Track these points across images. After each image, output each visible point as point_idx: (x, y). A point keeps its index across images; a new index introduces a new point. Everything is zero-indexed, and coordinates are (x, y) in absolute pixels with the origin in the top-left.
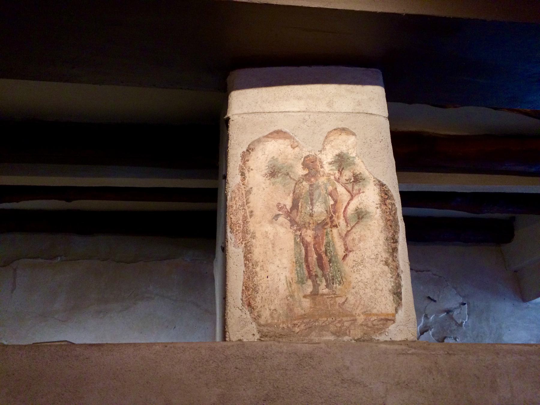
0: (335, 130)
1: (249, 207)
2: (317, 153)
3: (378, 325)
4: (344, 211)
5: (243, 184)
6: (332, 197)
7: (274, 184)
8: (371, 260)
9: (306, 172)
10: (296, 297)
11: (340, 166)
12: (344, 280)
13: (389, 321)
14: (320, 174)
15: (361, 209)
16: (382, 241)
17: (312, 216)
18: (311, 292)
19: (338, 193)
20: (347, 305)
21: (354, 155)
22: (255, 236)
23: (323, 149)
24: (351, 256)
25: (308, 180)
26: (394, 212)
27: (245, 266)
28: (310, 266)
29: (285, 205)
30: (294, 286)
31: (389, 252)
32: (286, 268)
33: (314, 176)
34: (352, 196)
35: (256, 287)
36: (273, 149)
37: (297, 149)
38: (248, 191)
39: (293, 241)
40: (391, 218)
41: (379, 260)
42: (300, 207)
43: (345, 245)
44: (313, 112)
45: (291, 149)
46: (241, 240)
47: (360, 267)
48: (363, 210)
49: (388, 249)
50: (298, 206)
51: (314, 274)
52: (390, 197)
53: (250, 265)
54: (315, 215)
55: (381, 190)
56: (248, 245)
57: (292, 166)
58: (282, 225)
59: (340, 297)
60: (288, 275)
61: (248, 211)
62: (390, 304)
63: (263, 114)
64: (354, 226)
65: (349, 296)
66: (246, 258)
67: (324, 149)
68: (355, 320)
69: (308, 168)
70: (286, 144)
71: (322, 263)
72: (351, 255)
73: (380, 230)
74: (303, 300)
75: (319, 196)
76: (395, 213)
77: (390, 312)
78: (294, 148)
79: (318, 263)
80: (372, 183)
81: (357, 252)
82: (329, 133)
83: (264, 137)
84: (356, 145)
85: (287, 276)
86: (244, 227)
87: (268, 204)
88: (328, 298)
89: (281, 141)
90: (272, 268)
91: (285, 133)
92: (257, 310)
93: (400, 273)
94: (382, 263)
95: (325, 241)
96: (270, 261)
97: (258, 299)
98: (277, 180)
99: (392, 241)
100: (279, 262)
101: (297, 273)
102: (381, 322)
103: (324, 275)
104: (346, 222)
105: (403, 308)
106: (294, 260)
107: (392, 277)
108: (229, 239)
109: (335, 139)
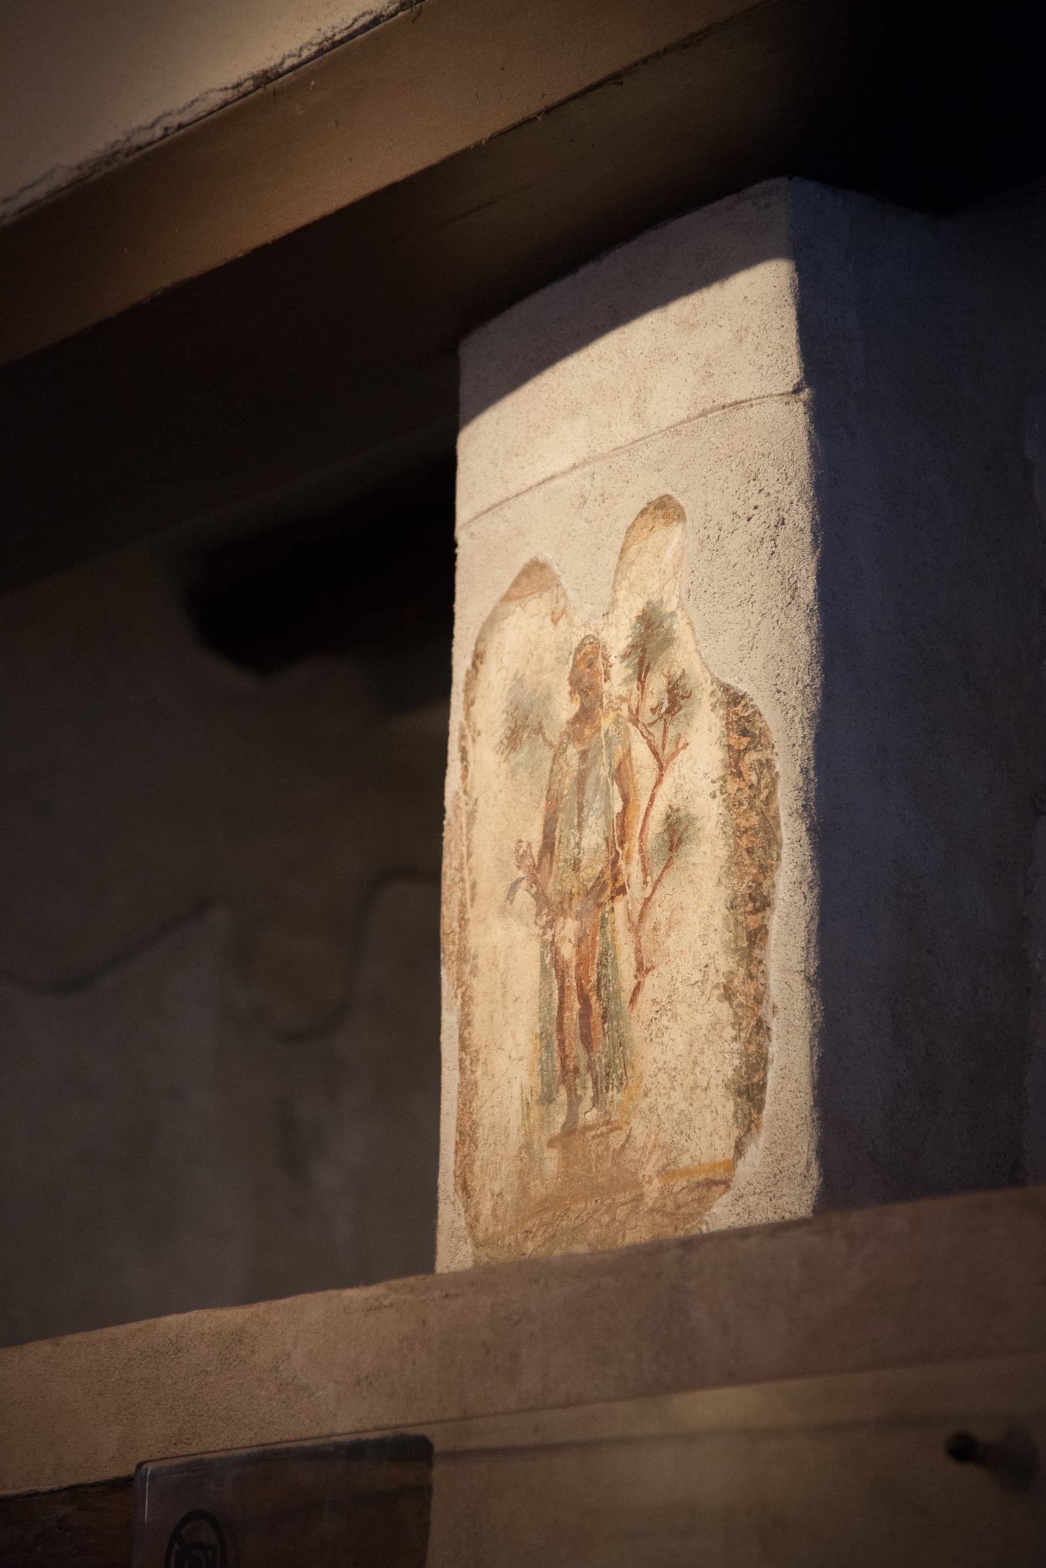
0: (643, 512)
3: (687, 1204)
6: (621, 786)
9: (575, 707)
13: (714, 1188)
17: (578, 870)
18: (564, 1126)
19: (632, 770)
20: (629, 1153)
26: (765, 793)
31: (736, 950)
32: (521, 1059)
39: (538, 964)
42: (557, 843)
43: (638, 950)
48: (682, 814)
49: (736, 937)
51: (571, 1067)
64: (659, 880)
67: (614, 603)
68: (639, 1198)
72: (649, 981)
73: (715, 876)
77: (720, 1159)
79: (581, 1027)
81: (661, 970)
84: (681, 559)
88: (593, 1137)
93: (769, 1018)
94: (716, 992)
99: (750, 906)
101: (542, 1069)
102: (695, 1195)
107: (735, 1039)
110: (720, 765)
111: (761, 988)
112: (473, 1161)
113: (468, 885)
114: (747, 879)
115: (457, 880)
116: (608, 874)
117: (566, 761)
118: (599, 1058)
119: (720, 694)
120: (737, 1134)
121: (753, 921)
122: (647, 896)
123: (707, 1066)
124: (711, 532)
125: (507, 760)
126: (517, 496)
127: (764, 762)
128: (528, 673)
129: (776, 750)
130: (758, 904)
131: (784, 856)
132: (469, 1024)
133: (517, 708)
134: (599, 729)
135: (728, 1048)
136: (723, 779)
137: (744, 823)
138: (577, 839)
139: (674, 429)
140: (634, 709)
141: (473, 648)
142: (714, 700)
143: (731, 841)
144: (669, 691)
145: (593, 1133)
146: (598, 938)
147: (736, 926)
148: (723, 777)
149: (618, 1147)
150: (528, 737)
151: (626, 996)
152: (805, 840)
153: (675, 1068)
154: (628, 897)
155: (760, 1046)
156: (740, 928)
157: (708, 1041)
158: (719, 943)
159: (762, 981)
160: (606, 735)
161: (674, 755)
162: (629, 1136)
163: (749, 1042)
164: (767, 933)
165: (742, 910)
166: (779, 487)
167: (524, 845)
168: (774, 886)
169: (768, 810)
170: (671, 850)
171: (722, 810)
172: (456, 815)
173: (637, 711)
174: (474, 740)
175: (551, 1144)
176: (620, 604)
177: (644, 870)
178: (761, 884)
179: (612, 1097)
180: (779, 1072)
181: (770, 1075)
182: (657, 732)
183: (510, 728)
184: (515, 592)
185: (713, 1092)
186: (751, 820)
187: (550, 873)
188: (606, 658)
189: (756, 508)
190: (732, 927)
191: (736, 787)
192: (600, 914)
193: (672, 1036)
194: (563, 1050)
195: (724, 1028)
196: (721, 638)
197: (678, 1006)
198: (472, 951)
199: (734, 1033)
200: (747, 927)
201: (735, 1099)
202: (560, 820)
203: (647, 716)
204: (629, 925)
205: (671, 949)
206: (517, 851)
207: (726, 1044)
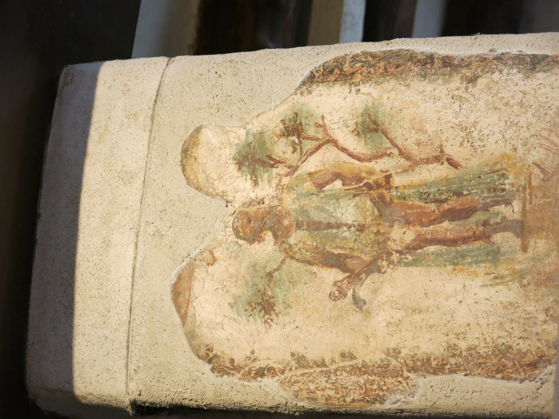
0: (184, 170)
1: (333, 361)
2: (230, 209)
4: (359, 159)
5: (283, 372)
6: (327, 183)
7: (288, 306)
9: (269, 236)
10: (523, 267)
11: (264, 164)
12: (498, 167)
14: (276, 207)
15: (357, 124)
16: (427, 86)
17: (364, 226)
18: (518, 236)
19: (320, 171)
20: (547, 165)
21: (242, 132)
22: (394, 350)
23: (222, 197)
24: (450, 150)
25: (287, 231)
26: (370, 59)
27: (454, 372)
28: (466, 234)
29: (335, 284)
30: (502, 270)
31: (450, 75)
32: (465, 287)
33: (279, 218)
34: (328, 142)
35: (500, 351)
36: (211, 304)
37: (218, 254)
38: (298, 363)
39: (410, 268)
40: (382, 64)
41: (465, 95)
43: (427, 161)
44: (140, 216)
45: (216, 265)
46: (400, 379)
47: (475, 134)
48: (360, 120)
49: (444, 75)
50: (340, 255)
51: (481, 228)
52: (339, 63)
53: (453, 361)
54: (361, 220)
55: (322, 82)
56: (411, 363)
57: (254, 266)
58: (375, 291)
59: (530, 177)
60: (479, 281)
61: (341, 364)
62: (553, 78)
63: (133, 324)
64: (391, 141)
65: (530, 159)
66: (439, 370)
67: (223, 196)
69: (261, 231)
70: (204, 275)
71: (462, 210)
72: (449, 150)
73: (404, 88)
74: (530, 254)
76: (373, 56)
78: (215, 260)
79: (459, 219)
81: (444, 139)
82: (189, 182)
83: (184, 324)
85: (481, 284)
86: (373, 373)
87: (330, 320)
88: (531, 203)
89: (197, 286)
90: (462, 315)
91: (179, 278)
92: (545, 349)
93: (495, 54)
94: (470, 90)
95: (418, 203)
96: (449, 317)
97: (524, 346)
98: (280, 298)
99: (428, 66)
100: (451, 300)
101: (476, 262)
103: (486, 208)
104: (381, 156)
106: (450, 268)
107: (501, 72)
108: (396, 406)
109: (204, 172)
110: (343, 87)
111: (477, 58)
114: (413, 67)
117: (296, 245)
119: (304, 88)
121: (438, 63)
123: (511, 94)
129: (349, 53)
130: (429, 61)
131: (408, 48)
143: (388, 78)
148: (350, 85)
149: (542, 176)
153: (506, 122)
156: (439, 72)
158: (442, 87)
163: (506, 64)
164: (447, 56)
168: (423, 53)
171: (368, 85)
179: (509, 184)
185: (528, 89)
187: (358, 257)
189: (216, 72)
190: (437, 77)
191: (359, 76)
192: (396, 201)
193: (486, 127)
194: (470, 237)
197: (469, 122)
199: (497, 72)
200: (439, 68)
201: (537, 72)
202: (329, 249)
205: (434, 129)
207: (503, 78)
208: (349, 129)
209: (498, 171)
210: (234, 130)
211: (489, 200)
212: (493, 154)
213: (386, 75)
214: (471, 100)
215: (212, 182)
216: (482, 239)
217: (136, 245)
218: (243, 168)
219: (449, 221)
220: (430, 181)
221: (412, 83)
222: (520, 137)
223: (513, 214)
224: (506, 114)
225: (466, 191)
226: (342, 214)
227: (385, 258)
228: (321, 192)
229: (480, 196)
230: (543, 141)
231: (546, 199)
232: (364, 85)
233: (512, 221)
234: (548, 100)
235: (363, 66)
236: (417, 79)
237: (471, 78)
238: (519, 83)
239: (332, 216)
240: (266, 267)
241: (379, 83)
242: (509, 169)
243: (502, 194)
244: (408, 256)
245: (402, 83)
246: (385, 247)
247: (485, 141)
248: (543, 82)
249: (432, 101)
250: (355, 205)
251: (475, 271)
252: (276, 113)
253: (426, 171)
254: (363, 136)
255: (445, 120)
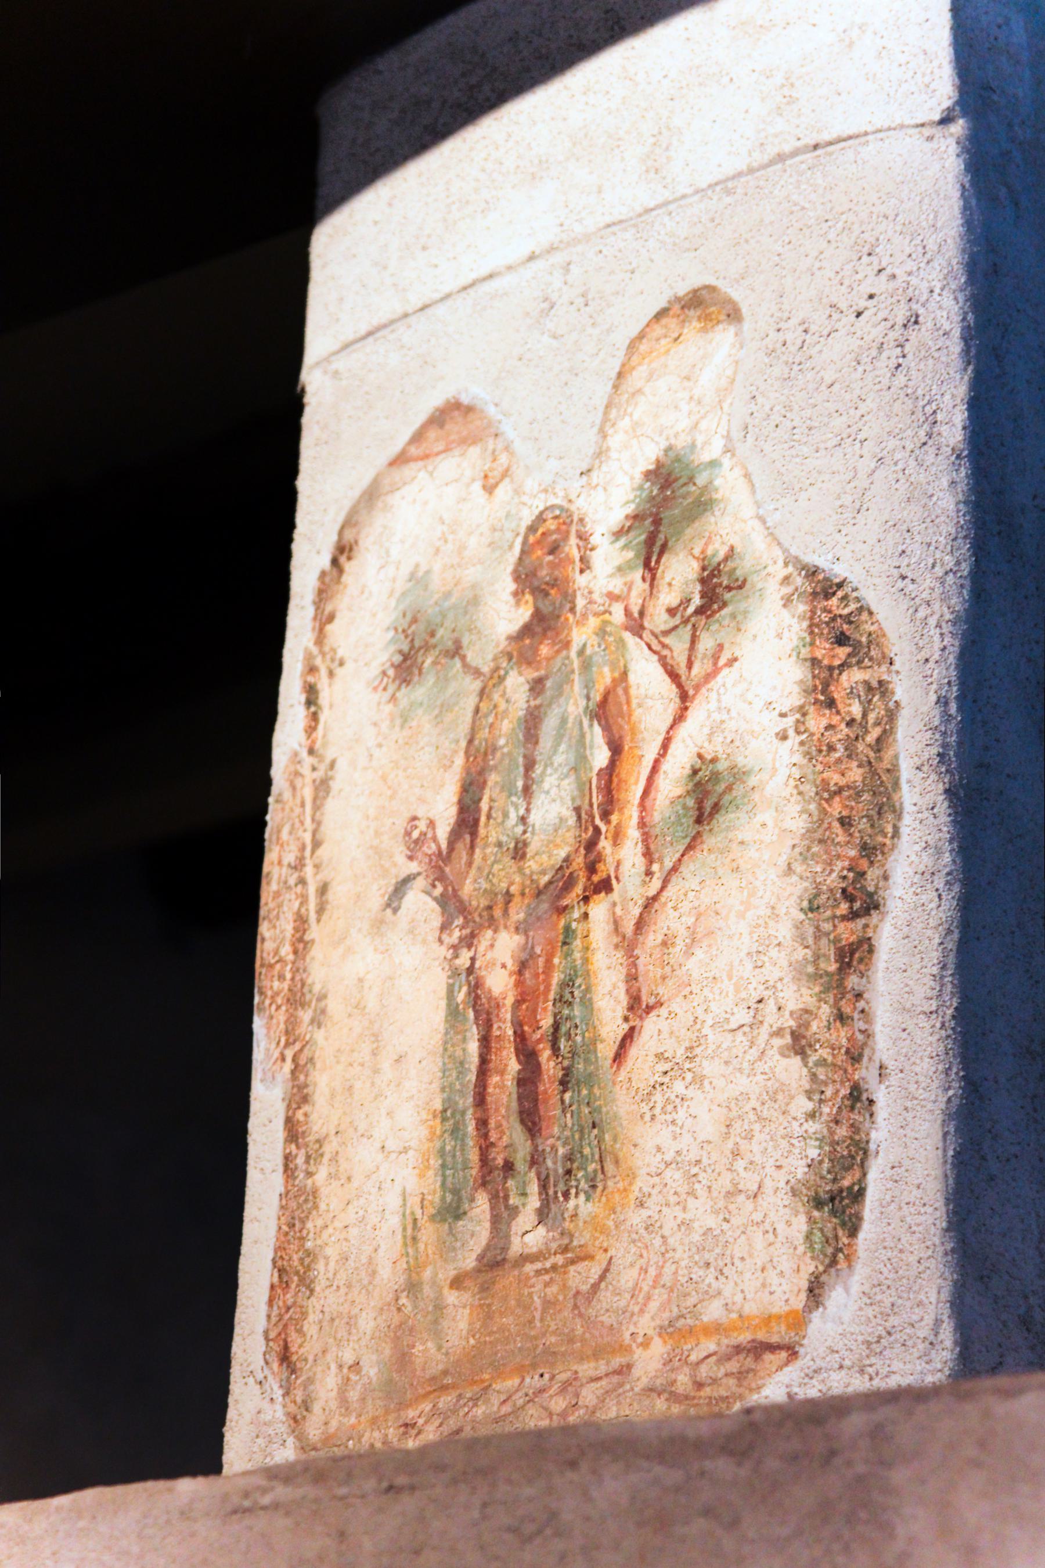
3: (715, 1381)
4: (646, 793)
6: (607, 729)
8: (727, 1040)
9: (524, 614)
12: (610, 1167)
13: (768, 1357)
17: (523, 856)
18: (480, 1258)
20: (605, 1296)
21: (713, 450)
26: (875, 733)
28: (492, 1124)
31: (816, 976)
32: (405, 1150)
39: (443, 1003)
41: (764, 1032)
42: (483, 819)
43: (632, 978)
48: (722, 766)
49: (817, 957)
51: (500, 1161)
64: (675, 869)
67: (601, 454)
72: (651, 1025)
75: (559, 738)
77: (779, 1307)
79: (519, 1098)
80: (773, 592)
81: (675, 1007)
85: (408, 1190)
88: (538, 1273)
94: (777, 1042)
99: (844, 907)
101: (443, 1166)
102: (733, 1366)
105: (859, 1277)
107: (812, 1115)
110: (796, 689)
111: (860, 1037)
112: (304, 1315)
113: (312, 890)
114: (839, 864)
115: (292, 881)
116: (579, 861)
118: (553, 1148)
119: (799, 581)
120: (812, 1269)
121: (848, 932)
122: (652, 892)
123: (758, 1158)
124: (789, 337)
125: (393, 698)
126: (422, 309)
127: (875, 684)
128: (437, 567)
130: (857, 905)
131: (904, 831)
132: (305, 1099)
133: (414, 620)
134: (567, 645)
135: (796, 1129)
136: (802, 711)
137: (835, 778)
138: (522, 812)
139: (724, 185)
140: (635, 611)
141: (335, 538)
142: (787, 590)
143: (813, 807)
144: (703, 581)
145: (539, 1265)
146: (556, 961)
147: (817, 938)
148: (801, 708)
149: (585, 1288)
150: (435, 663)
151: (606, 1050)
152: (943, 807)
153: (698, 1162)
154: (615, 896)
155: (855, 1128)
156: (824, 941)
157: (760, 1118)
158: (785, 964)
159: (862, 1026)
160: (581, 652)
161: (709, 677)
162: (607, 1270)
163: (837, 1122)
164: (871, 951)
165: (829, 913)
166: (910, 265)
167: (422, 826)
168: (886, 878)
169: (880, 759)
170: (699, 821)
171: (797, 758)
172: (294, 788)
173: (642, 613)
174: (331, 674)
175: (457, 1283)
176: (613, 454)
177: (648, 855)
178: (863, 874)
179: (577, 1207)
180: (889, 1173)
181: (873, 1175)
182: (679, 645)
183: (400, 652)
184: (413, 451)
186: (849, 774)
187: (470, 864)
188: (582, 537)
189: (871, 297)
190: (810, 941)
191: (824, 722)
192: (562, 923)
193: (692, 1111)
194: (486, 1136)
195: (792, 1098)
196: (804, 495)
197: (705, 1063)
198: (317, 988)
199: (809, 1106)
200: (837, 940)
202: (490, 784)
203: (658, 619)
204: (616, 940)
205: (695, 975)
206: (408, 834)
207: (795, 1124)
208: (706, 744)
209: (603, 1172)
210: (725, 418)
211: (549, 1163)
212: (635, 1146)
213: (822, 798)
214: (754, 1053)
215: (629, 410)
216: (482, 1167)
217: (532, 257)
218: (648, 484)
219: (519, 1072)
220: (595, 998)
221: (795, 878)
222: (664, 1209)
223: (520, 1233)
224: (715, 1156)
225: (572, 1097)
226: (548, 792)
227: (464, 932)
228: (591, 719)
229: (559, 1138)
230: (652, 1271)
231: (540, 1308)
232: (796, 747)
233: (507, 1237)
234: (737, 1262)
235: (850, 723)
236: (806, 890)
237: (804, 1037)
238: (783, 1171)
239: (546, 766)
240: (470, 630)
241: (802, 788)
242: (604, 1199)
243: (560, 1195)
244: (465, 989)
245: (797, 850)
246: (481, 927)
247: (664, 1117)
248: (780, 1238)
249: (755, 947)
250: (561, 819)
251: (428, 1168)
252: (751, 523)
253: (614, 979)
254: (690, 786)
255: (711, 997)
